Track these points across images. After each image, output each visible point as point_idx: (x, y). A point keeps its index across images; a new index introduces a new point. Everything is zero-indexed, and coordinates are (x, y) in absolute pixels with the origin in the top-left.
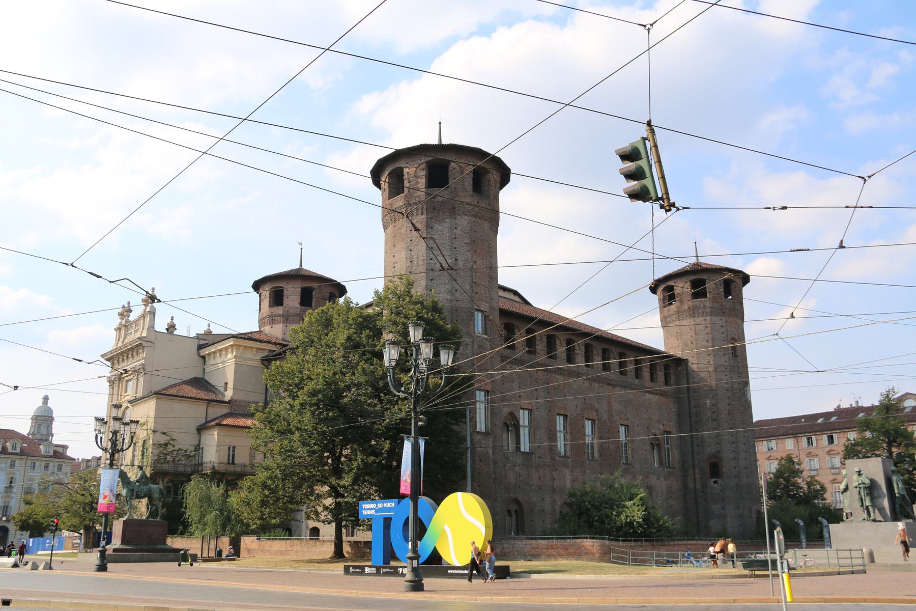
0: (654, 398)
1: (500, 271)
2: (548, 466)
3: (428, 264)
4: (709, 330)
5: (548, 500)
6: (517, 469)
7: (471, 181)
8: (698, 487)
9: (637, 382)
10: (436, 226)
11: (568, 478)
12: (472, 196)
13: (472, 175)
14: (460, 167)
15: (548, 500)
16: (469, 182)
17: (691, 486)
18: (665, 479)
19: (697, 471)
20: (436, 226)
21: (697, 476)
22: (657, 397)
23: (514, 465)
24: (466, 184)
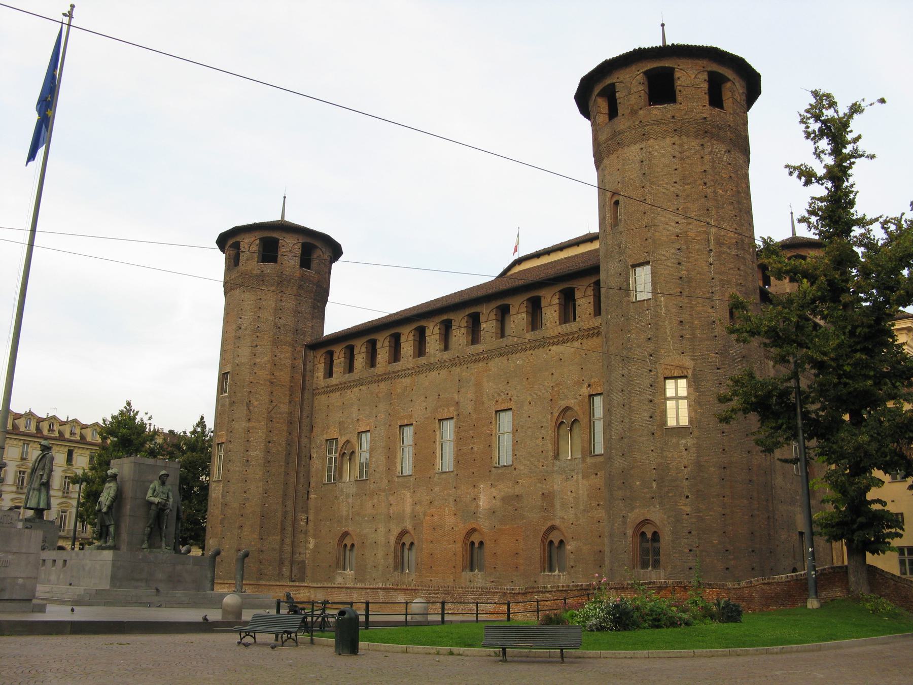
0: (566, 350)
2: (384, 491)
5: (382, 530)
6: (350, 500)
11: (409, 501)
15: (382, 530)
22: (576, 344)
23: (348, 496)
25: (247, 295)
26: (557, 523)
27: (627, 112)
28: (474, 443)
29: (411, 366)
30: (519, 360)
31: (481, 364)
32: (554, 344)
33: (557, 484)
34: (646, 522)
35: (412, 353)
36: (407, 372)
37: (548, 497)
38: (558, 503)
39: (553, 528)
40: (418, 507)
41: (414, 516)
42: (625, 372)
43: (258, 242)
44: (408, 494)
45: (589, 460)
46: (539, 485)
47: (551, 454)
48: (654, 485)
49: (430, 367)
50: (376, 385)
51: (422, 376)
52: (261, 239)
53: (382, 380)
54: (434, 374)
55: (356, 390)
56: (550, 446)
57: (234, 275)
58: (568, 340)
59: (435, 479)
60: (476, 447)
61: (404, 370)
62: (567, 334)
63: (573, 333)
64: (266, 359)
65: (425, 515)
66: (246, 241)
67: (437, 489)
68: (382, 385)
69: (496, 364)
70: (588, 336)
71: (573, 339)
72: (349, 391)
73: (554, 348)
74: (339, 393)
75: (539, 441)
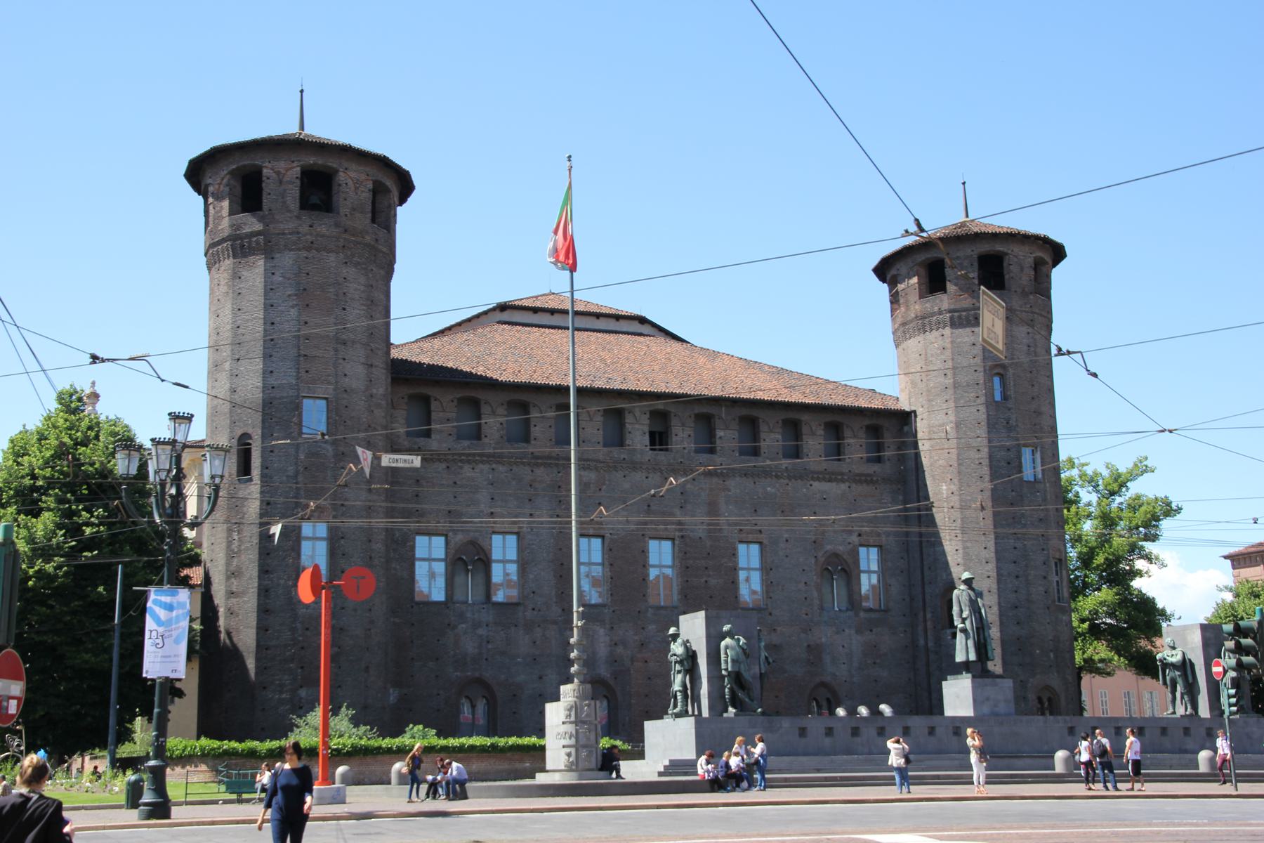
0: (834, 489)
1: (394, 325)
2: (555, 623)
3: (235, 335)
4: (948, 353)
7: (297, 194)
8: (931, 644)
9: (786, 463)
10: (245, 273)
12: (298, 217)
13: (298, 182)
14: (278, 173)
16: (293, 192)
17: (922, 642)
18: (858, 632)
19: (929, 616)
20: (245, 273)
21: (929, 623)
22: (844, 486)
23: (477, 625)
24: (289, 199)
25: (350, 272)
26: (828, 679)
27: (1019, 290)
28: (709, 576)
29: (601, 457)
30: (770, 487)
31: (715, 480)
32: (818, 479)
33: (824, 635)
34: (1047, 688)
35: (601, 439)
36: (592, 464)
37: (815, 651)
38: (827, 659)
39: (823, 684)
40: (620, 650)
41: (613, 660)
42: (1019, 545)
43: (370, 186)
44: (602, 631)
45: (862, 614)
46: (803, 635)
47: (817, 602)
48: (1052, 655)
49: (634, 466)
50: (528, 469)
51: (620, 474)
52: (375, 182)
53: (537, 465)
54: (638, 476)
55: (486, 467)
56: (815, 594)
57: (324, 226)
58: (836, 480)
59: (649, 615)
60: (713, 582)
61: (588, 460)
62: (833, 473)
63: (842, 474)
64: (381, 391)
65: (632, 660)
66: (352, 174)
67: (652, 627)
68: (540, 471)
69: (734, 484)
70: (860, 482)
71: (843, 481)
72: (467, 467)
73: (816, 484)
74: (444, 465)
75: (802, 586)
